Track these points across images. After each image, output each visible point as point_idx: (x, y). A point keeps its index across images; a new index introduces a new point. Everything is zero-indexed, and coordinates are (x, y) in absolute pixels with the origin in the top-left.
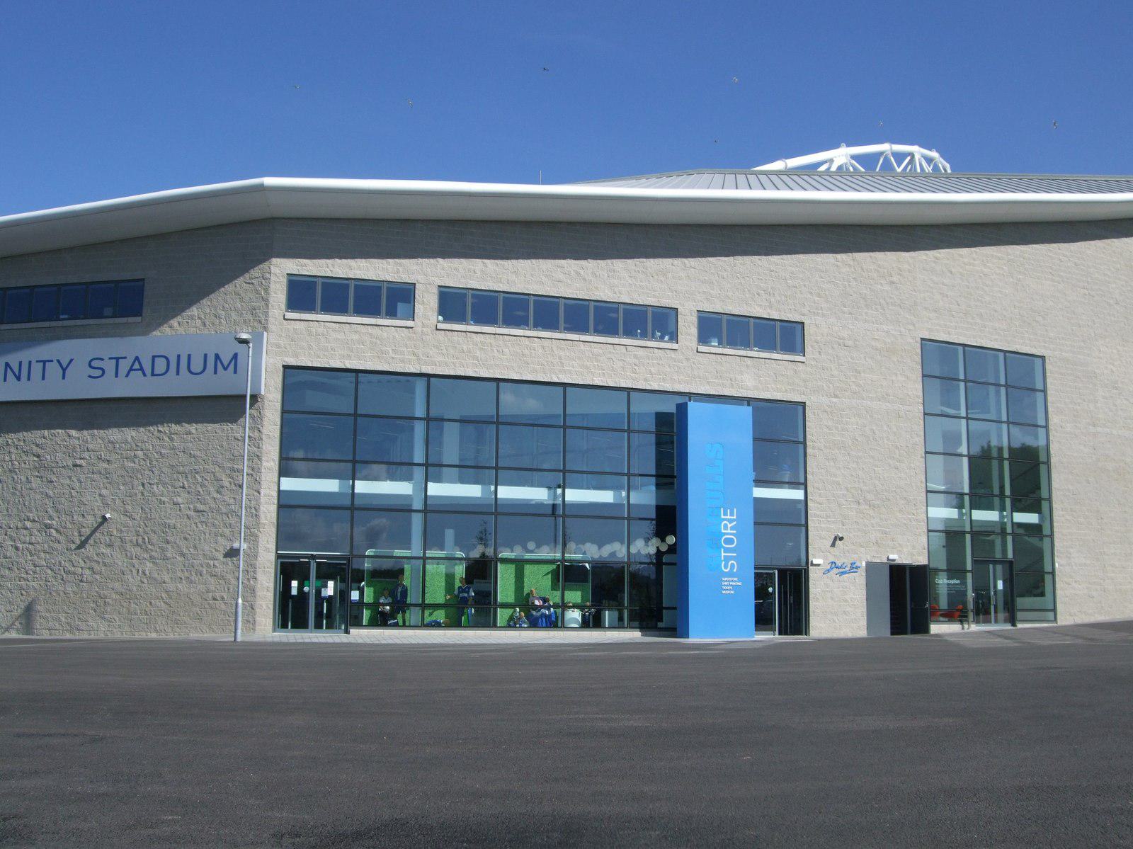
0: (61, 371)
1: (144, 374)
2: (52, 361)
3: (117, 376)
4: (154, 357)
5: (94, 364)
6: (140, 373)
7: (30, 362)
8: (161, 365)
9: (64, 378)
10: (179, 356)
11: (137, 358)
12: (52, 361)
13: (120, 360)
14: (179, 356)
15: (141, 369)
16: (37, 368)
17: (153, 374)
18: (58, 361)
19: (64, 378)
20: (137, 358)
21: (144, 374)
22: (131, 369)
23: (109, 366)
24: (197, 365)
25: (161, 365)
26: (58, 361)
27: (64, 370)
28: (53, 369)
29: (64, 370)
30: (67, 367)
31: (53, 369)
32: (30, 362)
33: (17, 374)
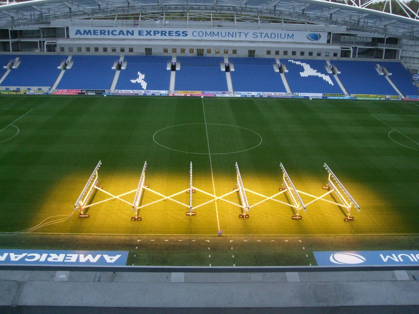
0: (245, 36)
1: (269, 38)
2: (242, 32)
3: (261, 38)
4: (271, 34)
5: (255, 34)
6: (268, 37)
7: (236, 33)
8: (273, 36)
9: (246, 37)
10: (278, 34)
11: (267, 33)
12: (242, 32)
13: (262, 34)
14: (278, 34)
15: (268, 36)
16: (238, 34)
17: (271, 38)
18: (244, 33)
19: (246, 37)
20: (267, 33)
21: (269, 38)
22: (265, 36)
23: (259, 35)
24: (283, 36)
25: (273, 36)
26: (244, 33)
27: (246, 35)
28: (243, 35)
29: (246, 35)
30: (247, 34)
31: (243, 35)
32: (236, 33)
33: (232, 35)
